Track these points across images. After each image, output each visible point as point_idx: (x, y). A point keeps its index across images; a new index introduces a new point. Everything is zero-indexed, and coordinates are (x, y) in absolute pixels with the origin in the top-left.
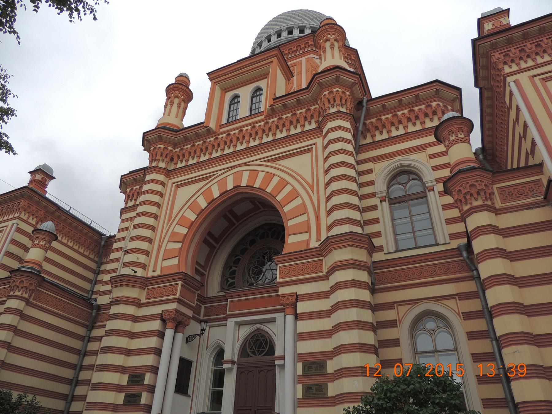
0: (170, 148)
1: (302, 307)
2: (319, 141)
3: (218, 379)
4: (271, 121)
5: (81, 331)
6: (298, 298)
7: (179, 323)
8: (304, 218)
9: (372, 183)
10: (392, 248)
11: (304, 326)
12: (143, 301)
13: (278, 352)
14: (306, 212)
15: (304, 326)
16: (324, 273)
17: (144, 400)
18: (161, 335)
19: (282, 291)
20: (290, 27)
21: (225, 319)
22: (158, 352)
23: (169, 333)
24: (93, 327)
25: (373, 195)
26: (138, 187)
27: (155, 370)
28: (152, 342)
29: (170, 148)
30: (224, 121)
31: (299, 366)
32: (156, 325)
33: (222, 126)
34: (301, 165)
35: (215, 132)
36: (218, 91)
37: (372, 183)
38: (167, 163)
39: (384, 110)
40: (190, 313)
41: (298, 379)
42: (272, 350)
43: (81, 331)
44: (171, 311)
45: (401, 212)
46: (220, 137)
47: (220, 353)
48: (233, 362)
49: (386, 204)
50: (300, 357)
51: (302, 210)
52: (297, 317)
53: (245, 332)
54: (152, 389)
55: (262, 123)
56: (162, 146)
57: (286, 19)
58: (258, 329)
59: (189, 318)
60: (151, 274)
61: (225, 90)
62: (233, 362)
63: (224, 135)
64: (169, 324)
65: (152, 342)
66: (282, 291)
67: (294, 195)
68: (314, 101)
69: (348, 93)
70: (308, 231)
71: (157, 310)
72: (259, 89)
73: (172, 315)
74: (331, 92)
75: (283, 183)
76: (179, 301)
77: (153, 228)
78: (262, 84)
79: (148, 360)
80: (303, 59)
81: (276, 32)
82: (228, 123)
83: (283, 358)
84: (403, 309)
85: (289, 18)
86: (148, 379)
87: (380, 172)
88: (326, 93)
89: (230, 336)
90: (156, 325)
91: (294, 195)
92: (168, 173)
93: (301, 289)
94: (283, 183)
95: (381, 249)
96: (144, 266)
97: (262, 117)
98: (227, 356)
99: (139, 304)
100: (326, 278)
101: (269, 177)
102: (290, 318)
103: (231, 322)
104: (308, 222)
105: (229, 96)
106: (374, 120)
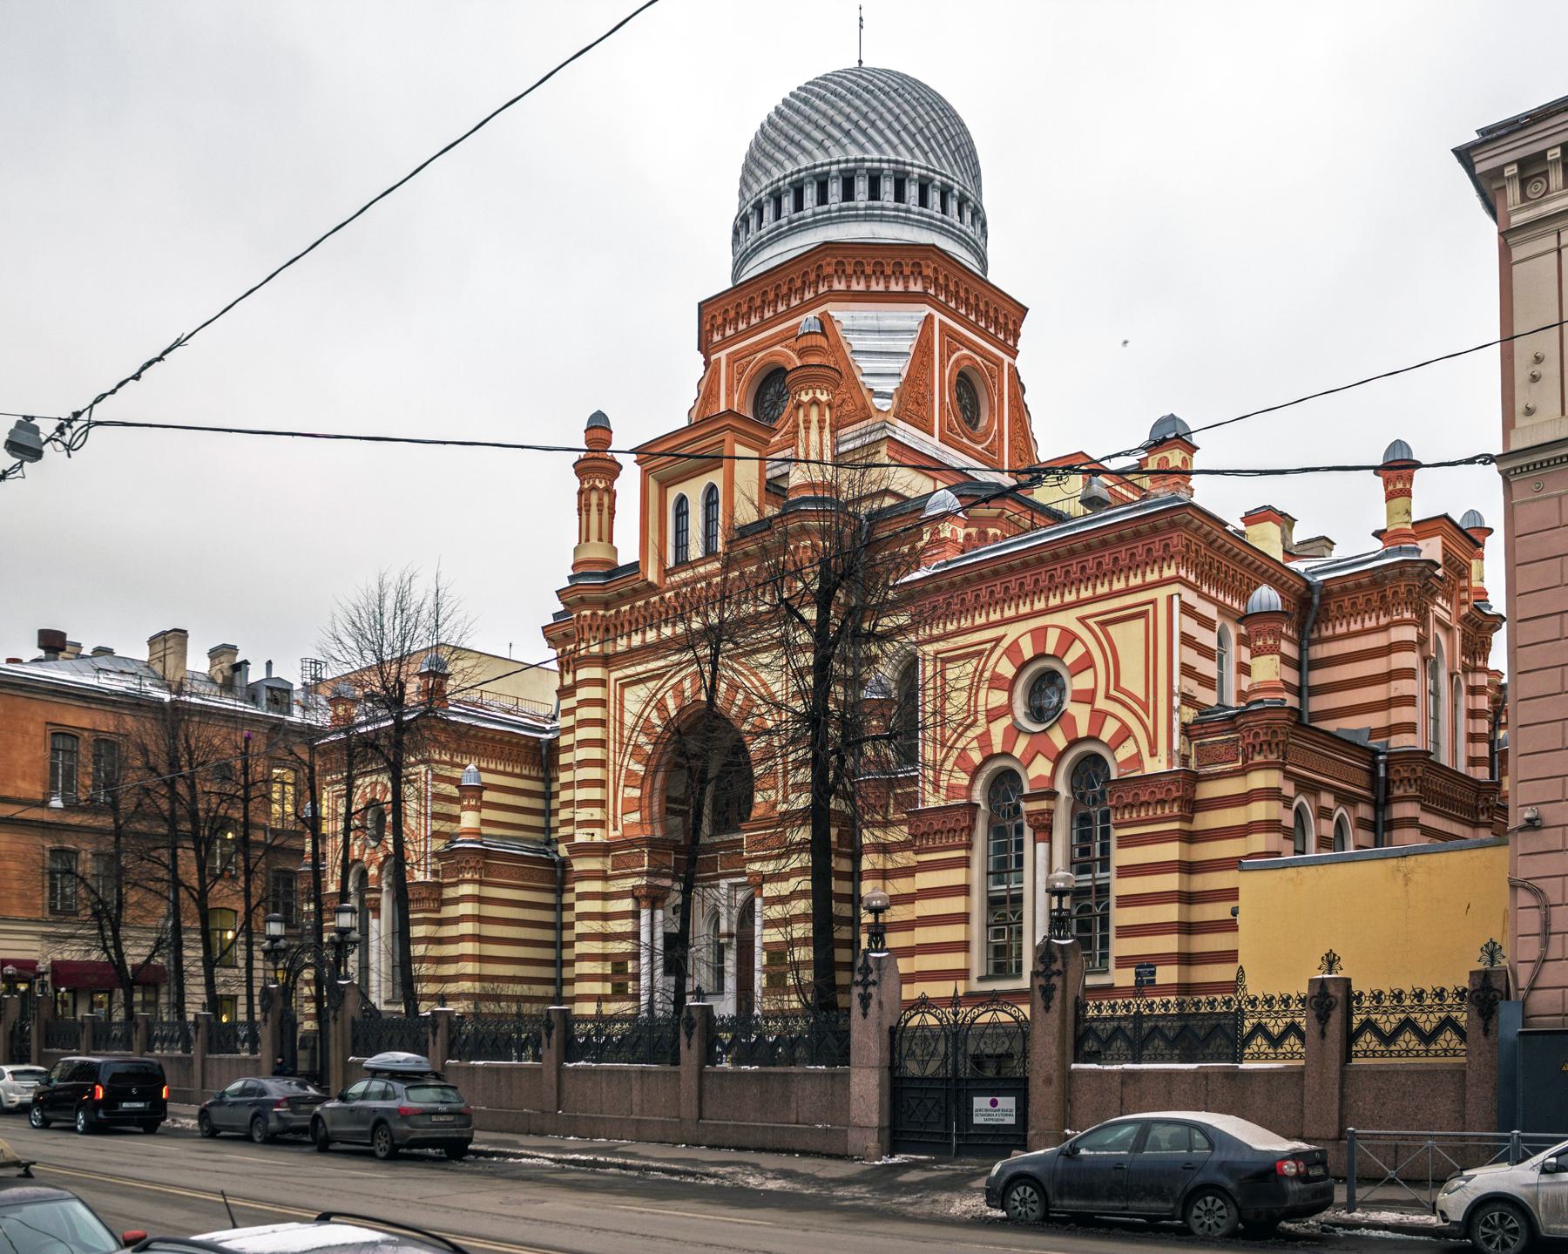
0: (601, 612)
5: (549, 898)
29: (601, 612)
30: (671, 562)
32: (627, 905)
36: (653, 487)
38: (602, 642)
43: (549, 898)
46: (668, 595)
56: (588, 613)
60: (612, 834)
61: (664, 484)
64: (643, 903)
71: (628, 884)
73: (643, 892)
76: (648, 874)
77: (602, 764)
92: (606, 661)
96: (601, 824)
99: (604, 877)
105: (673, 494)
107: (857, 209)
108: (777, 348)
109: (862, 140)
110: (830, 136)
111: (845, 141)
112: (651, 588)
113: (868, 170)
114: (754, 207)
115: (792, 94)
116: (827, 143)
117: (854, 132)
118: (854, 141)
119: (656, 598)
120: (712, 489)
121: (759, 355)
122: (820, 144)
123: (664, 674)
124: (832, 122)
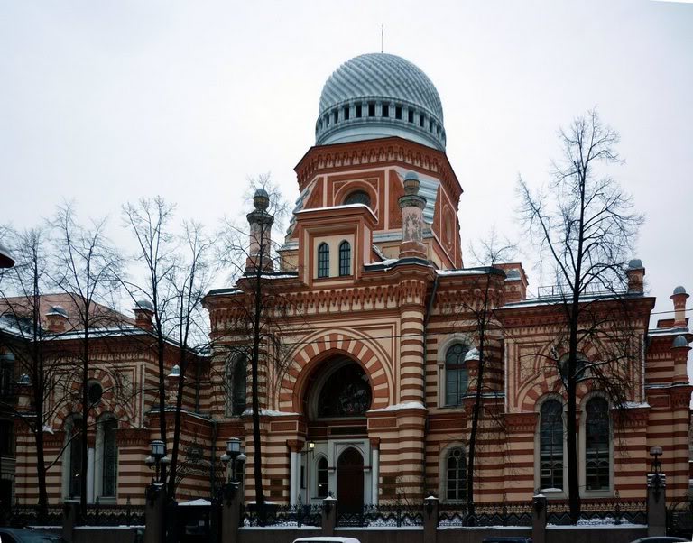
1: (383, 447)
2: (398, 320)
3: (323, 477)
4: (359, 289)
6: (380, 441)
7: (298, 447)
8: (385, 386)
9: (435, 352)
10: (443, 404)
11: (384, 458)
12: (270, 431)
13: (366, 463)
14: (387, 381)
15: (384, 458)
16: (397, 427)
17: (285, 493)
18: (288, 455)
19: (370, 435)
20: (372, 101)
21: (327, 439)
22: (288, 466)
23: (293, 455)
24: (217, 440)
25: (434, 362)
26: (226, 309)
27: (288, 477)
28: (284, 460)
30: (315, 276)
31: (381, 479)
32: (284, 449)
33: (313, 281)
34: (384, 339)
35: (308, 287)
37: (435, 352)
39: (452, 287)
40: (303, 439)
41: (379, 486)
42: (360, 459)
43: (208, 443)
44: (294, 441)
45: (454, 374)
46: (314, 292)
47: (323, 462)
48: (334, 469)
49: (443, 371)
50: (380, 475)
51: (383, 379)
52: (380, 452)
53: (341, 449)
54: (288, 488)
55: (352, 289)
57: (367, 81)
58: (351, 448)
59: (303, 442)
62: (334, 469)
63: (318, 292)
65: (284, 460)
66: (370, 435)
67: (378, 365)
68: (396, 281)
69: (422, 282)
70: (388, 396)
71: (283, 439)
72: (345, 242)
74: (409, 282)
75: (370, 354)
76: (298, 434)
78: (350, 238)
79: (283, 471)
80: (387, 169)
81: (355, 103)
82: (320, 278)
83: (370, 468)
84: (443, 445)
85: (371, 80)
86: (285, 482)
87: (443, 342)
88: (405, 281)
89: (332, 450)
90: (284, 449)
91: (378, 365)
93: (383, 436)
94: (370, 354)
95: (434, 405)
97: (352, 282)
98: (331, 464)
100: (398, 430)
101: (359, 345)
102: (375, 453)
103: (331, 442)
104: (388, 389)
105: (318, 241)
106: (443, 293)
107: (375, 120)
108: (362, 180)
109: (361, 87)
110: (388, 84)
111: (396, 89)
112: (304, 287)
113: (409, 107)
114: (332, 111)
115: (346, 64)
116: (388, 88)
117: (402, 87)
118: (401, 91)
119: (307, 293)
120: (345, 242)
121: (350, 182)
122: (384, 87)
123: (311, 332)
124: (390, 77)
